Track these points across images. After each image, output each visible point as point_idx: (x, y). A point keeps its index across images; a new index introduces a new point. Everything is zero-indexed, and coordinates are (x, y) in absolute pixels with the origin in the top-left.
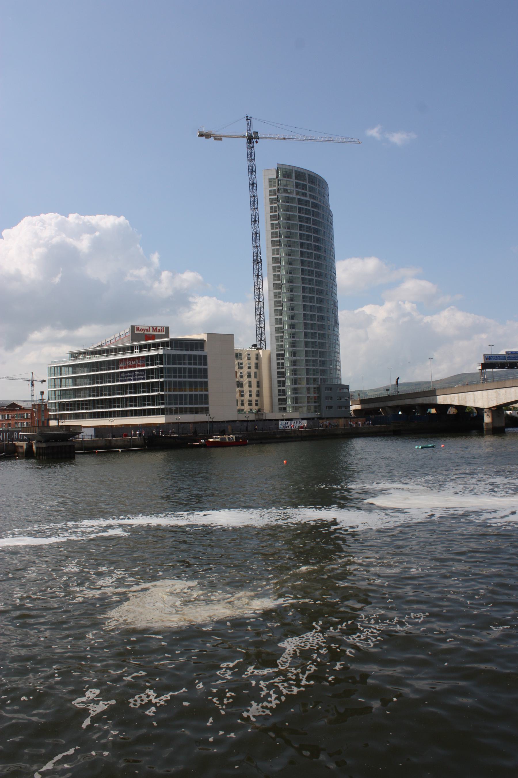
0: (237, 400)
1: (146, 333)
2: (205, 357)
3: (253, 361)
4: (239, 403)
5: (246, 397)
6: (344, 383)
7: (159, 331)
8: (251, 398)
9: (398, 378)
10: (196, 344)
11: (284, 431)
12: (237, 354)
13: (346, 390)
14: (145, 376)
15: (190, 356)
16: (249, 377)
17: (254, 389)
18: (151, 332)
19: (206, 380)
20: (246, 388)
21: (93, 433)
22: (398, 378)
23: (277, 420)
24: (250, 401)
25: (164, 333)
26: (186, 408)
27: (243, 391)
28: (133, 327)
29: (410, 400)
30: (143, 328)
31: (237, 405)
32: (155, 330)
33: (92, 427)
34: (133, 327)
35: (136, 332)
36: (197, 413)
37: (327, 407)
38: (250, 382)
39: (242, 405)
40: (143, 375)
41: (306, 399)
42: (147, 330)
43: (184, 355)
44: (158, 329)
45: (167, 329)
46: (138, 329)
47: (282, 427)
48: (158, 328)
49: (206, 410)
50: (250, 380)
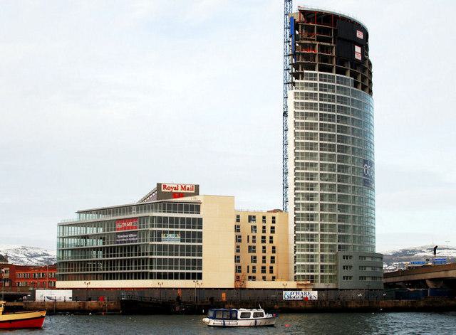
0: (248, 267)
1: (174, 191)
2: (200, 220)
3: (269, 224)
4: (251, 269)
5: (259, 264)
6: (377, 251)
7: (188, 190)
8: (264, 265)
10: (192, 207)
11: (288, 302)
12: (250, 217)
13: (378, 260)
15: (183, 219)
16: (264, 241)
17: (269, 255)
18: (179, 191)
23: (282, 290)
24: (264, 268)
25: (194, 192)
26: (177, 274)
27: (255, 257)
28: (159, 185)
29: (433, 274)
30: (170, 186)
31: (248, 272)
32: (184, 188)
33: (70, 289)
34: (159, 185)
35: (163, 190)
36: (188, 278)
37: (344, 277)
38: (264, 247)
39: (254, 271)
40: (135, 237)
41: (319, 268)
42: (175, 189)
43: (177, 218)
44: (187, 187)
45: (197, 187)
46: (165, 186)
47: (286, 296)
48: (187, 187)
49: (200, 276)
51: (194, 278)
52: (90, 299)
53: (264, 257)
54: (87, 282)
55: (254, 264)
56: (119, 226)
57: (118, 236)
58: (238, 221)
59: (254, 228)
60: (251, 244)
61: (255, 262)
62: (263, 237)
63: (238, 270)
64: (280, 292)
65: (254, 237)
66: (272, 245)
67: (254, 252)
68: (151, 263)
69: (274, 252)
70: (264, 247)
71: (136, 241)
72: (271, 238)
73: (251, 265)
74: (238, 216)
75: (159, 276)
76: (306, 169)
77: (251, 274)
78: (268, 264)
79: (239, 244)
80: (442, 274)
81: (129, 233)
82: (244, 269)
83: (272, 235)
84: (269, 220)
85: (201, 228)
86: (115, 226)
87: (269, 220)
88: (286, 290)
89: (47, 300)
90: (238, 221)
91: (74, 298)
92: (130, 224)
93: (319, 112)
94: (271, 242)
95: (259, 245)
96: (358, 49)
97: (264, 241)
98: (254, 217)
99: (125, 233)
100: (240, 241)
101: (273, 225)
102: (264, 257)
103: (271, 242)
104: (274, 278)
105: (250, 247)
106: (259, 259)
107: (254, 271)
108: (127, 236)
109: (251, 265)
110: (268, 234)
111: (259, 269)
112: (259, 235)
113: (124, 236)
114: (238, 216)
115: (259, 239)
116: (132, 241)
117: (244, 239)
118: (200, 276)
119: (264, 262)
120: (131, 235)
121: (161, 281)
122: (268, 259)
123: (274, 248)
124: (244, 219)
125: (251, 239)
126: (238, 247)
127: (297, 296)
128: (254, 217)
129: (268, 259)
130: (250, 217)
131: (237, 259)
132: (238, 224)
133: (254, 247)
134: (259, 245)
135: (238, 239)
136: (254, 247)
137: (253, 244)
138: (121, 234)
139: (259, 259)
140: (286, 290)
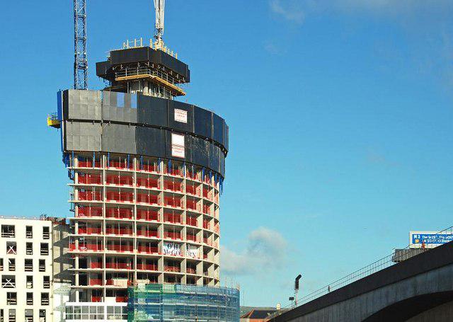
0: (2, 310)
8: (30, 307)
9: (300, 276)
17: (38, 289)
20: (21, 288)
22: (300, 276)
38: (30, 279)
50: (29, 274)
65: (13, 261)
70: (30, 279)
72: (42, 262)
78: (37, 304)
95: (20, 273)
106: (21, 298)
110: (36, 256)
112: (21, 256)
115: (20, 265)
122: (37, 298)
129: (37, 298)
134: (20, 273)
139: (21, 298)
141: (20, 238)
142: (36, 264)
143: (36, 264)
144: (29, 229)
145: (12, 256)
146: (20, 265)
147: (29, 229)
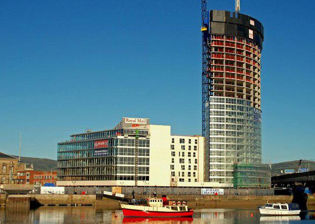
3: (193, 144)
4: (181, 174)
5: (186, 171)
8: (189, 171)
11: (204, 196)
12: (181, 140)
14: (108, 153)
16: (189, 156)
17: (193, 164)
19: (148, 157)
20: (186, 164)
21: (64, 191)
23: (200, 188)
27: (184, 166)
38: (190, 160)
39: (183, 176)
47: (204, 192)
49: (148, 178)
50: (190, 158)
51: (144, 180)
52: (76, 193)
53: (190, 166)
54: (74, 182)
55: (183, 171)
56: (96, 145)
57: (96, 152)
58: (173, 142)
59: (183, 147)
60: (181, 157)
61: (184, 169)
62: (189, 153)
63: (173, 174)
64: (199, 189)
66: (195, 158)
67: (183, 162)
68: (116, 170)
69: (196, 163)
70: (190, 160)
71: (107, 155)
72: (194, 153)
73: (181, 171)
74: (173, 139)
75: (121, 178)
76: (217, 135)
77: (182, 178)
79: (173, 157)
80: (305, 178)
81: (102, 149)
82: (177, 174)
83: (195, 151)
84: (193, 142)
85: (148, 146)
86: (94, 145)
87: (193, 142)
88: (205, 188)
89: (48, 193)
90: (173, 142)
91: (66, 193)
92: (103, 143)
93: (225, 137)
94: (194, 156)
95: (186, 158)
96: (251, 32)
97: (189, 156)
98: (184, 140)
99: (100, 149)
100: (174, 155)
101: (196, 145)
102: (190, 166)
103: (194, 156)
104: (196, 180)
105: (180, 160)
106: (187, 167)
107: (183, 176)
108: (101, 151)
109: (181, 171)
110: (192, 151)
111: (186, 174)
112: (186, 151)
113: (99, 151)
114: (173, 139)
115: (186, 154)
116: (104, 155)
117: (177, 154)
118: (148, 178)
119: (190, 169)
120: (104, 151)
121: (123, 181)
122: (192, 167)
123: (196, 160)
124: (177, 139)
125: (181, 154)
126: (173, 159)
127: (210, 192)
128: (184, 140)
129: (192, 167)
130: (181, 140)
131: (172, 167)
132: (173, 144)
133: (183, 159)
134: (186, 158)
135: (173, 154)
136: (183, 159)
137: (183, 158)
138: (98, 150)
139: (187, 167)
140: (205, 188)
141: (186, 144)
142: (192, 154)
143: (192, 154)
144: (190, 140)
145: (183, 151)
146: (186, 154)
147: (190, 140)
